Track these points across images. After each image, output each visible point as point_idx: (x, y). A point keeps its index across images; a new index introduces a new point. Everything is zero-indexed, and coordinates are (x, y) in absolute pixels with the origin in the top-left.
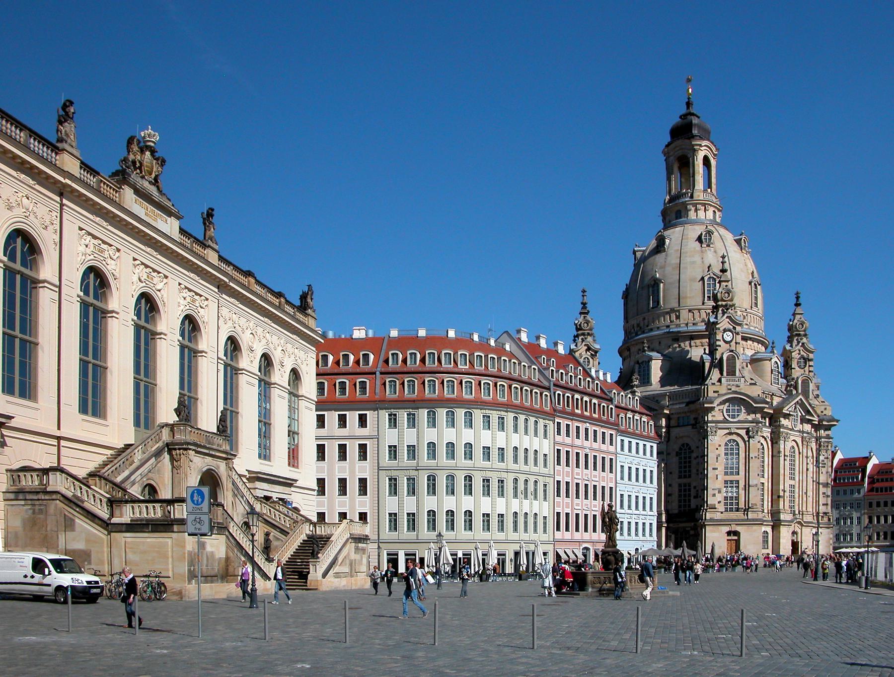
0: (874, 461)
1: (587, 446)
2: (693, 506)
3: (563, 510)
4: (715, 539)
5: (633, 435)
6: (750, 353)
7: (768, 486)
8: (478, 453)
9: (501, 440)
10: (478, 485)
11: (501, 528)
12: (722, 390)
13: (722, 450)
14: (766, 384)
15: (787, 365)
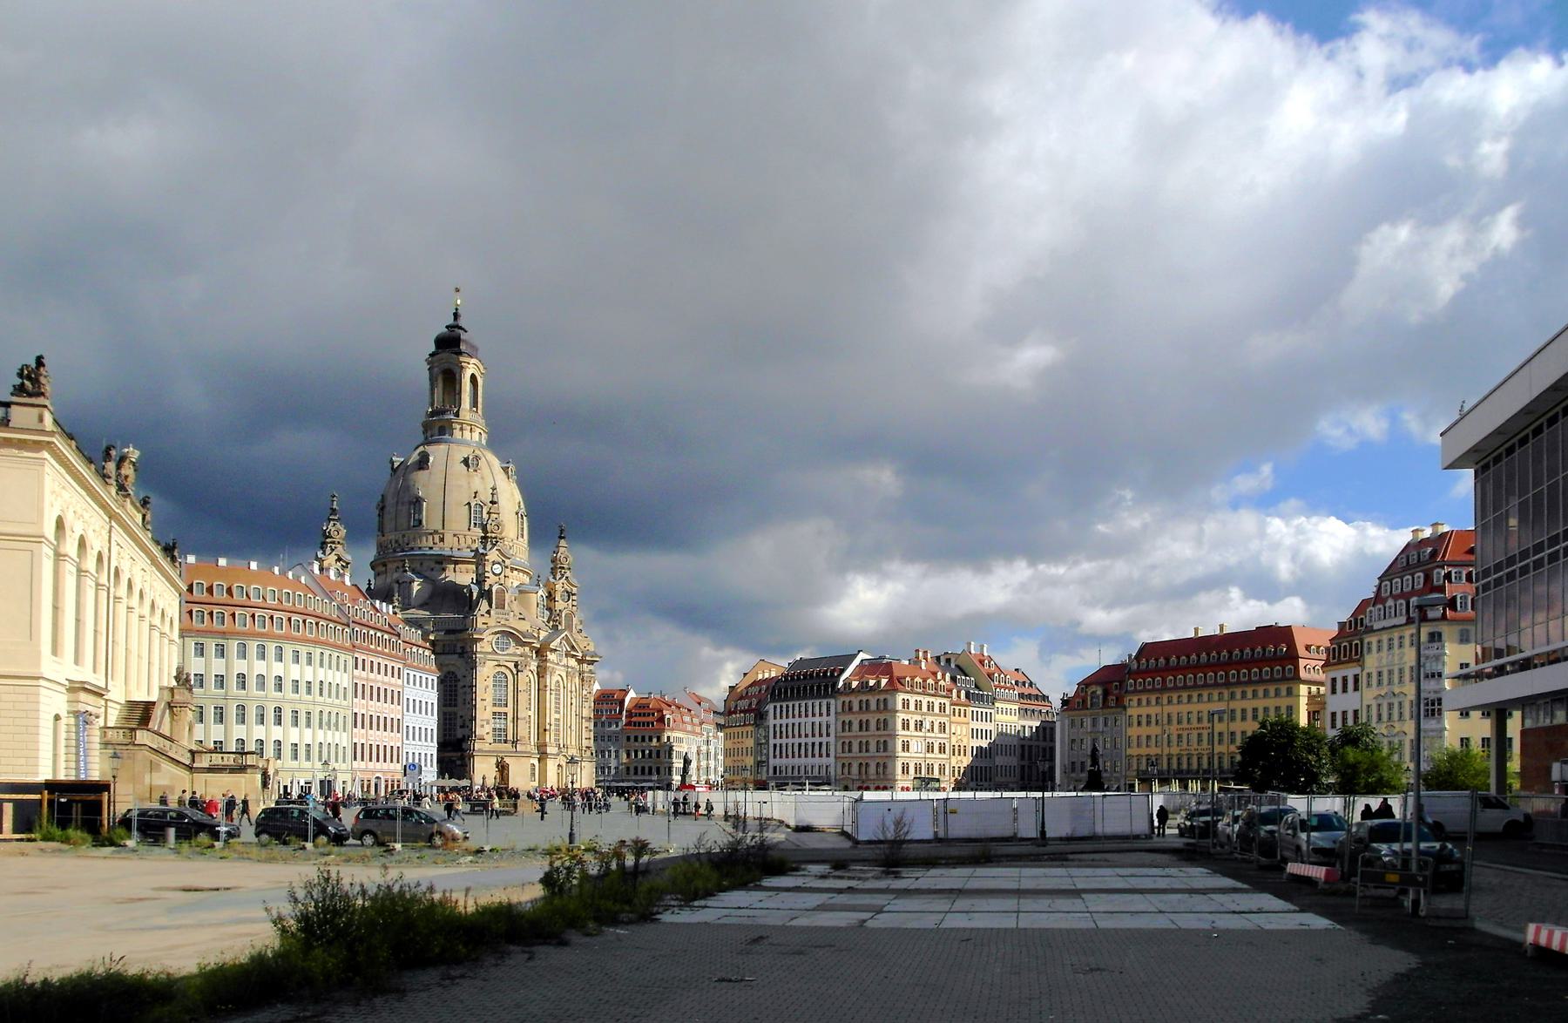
0: (632, 694)
1: (379, 680)
2: (460, 736)
3: (359, 740)
4: (483, 771)
5: (417, 668)
6: (516, 584)
7: (534, 719)
8: (287, 686)
9: (308, 673)
10: (287, 716)
11: (308, 758)
12: (492, 622)
13: (490, 682)
14: (532, 620)
15: (551, 597)
